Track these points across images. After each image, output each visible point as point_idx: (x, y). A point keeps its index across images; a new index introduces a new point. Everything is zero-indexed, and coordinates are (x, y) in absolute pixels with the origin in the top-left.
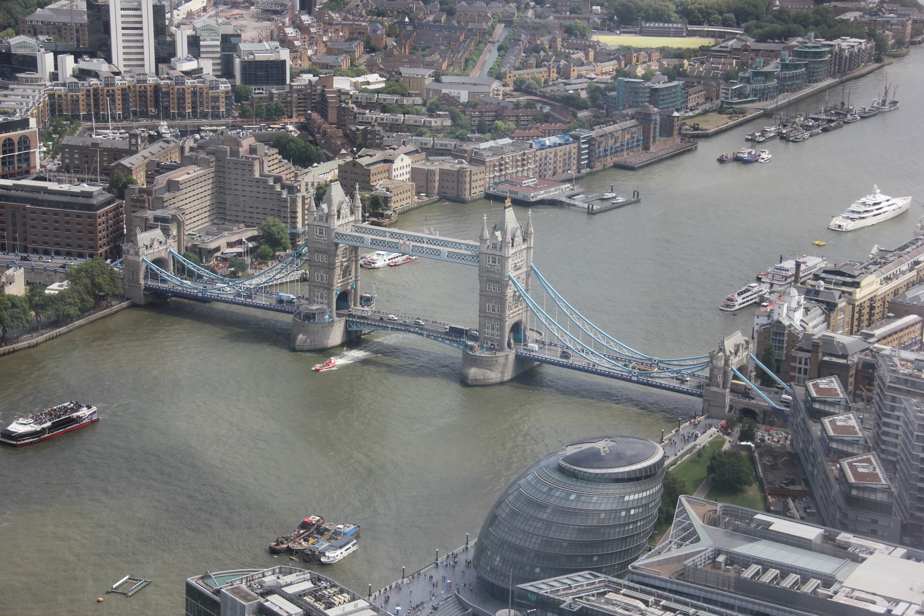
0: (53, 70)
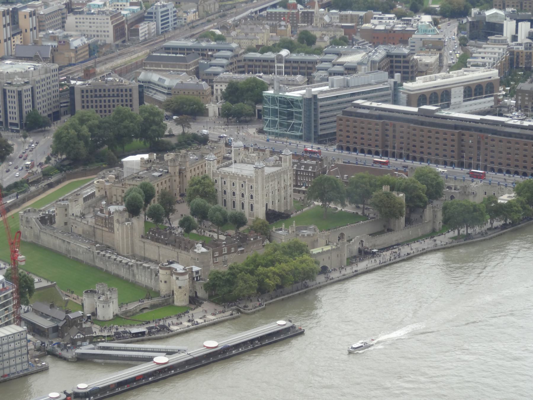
0: (514, 33)
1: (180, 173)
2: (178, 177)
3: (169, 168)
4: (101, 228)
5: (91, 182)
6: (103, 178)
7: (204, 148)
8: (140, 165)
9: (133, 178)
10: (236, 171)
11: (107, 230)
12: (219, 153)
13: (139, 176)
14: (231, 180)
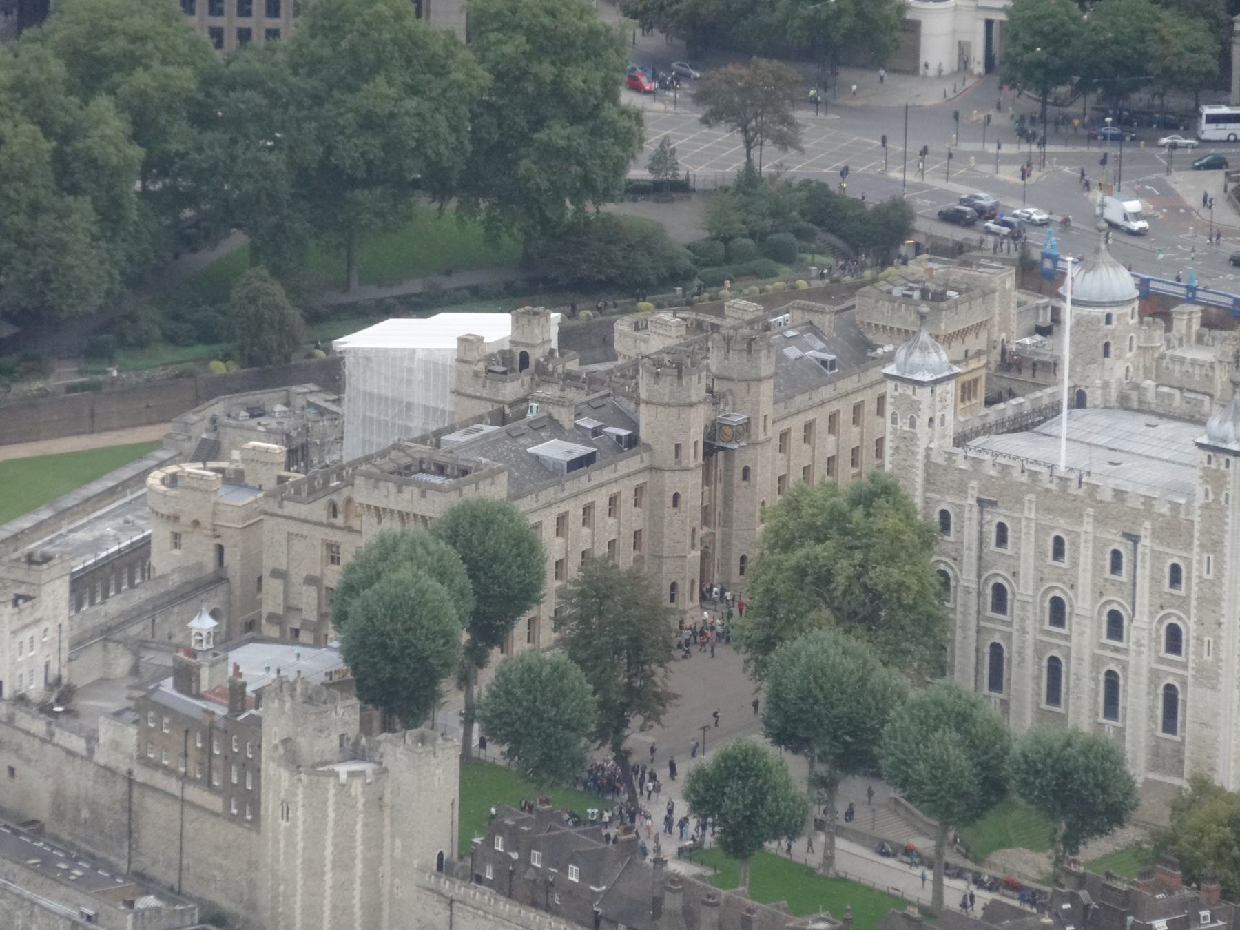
1: (710, 450)
2: (696, 479)
3: (645, 416)
4: (173, 786)
5: (127, 473)
6: (208, 451)
7: (883, 298)
8: (451, 382)
9: (404, 473)
10: (1083, 464)
11: (215, 803)
12: (977, 328)
13: (440, 456)
14: (1047, 520)
